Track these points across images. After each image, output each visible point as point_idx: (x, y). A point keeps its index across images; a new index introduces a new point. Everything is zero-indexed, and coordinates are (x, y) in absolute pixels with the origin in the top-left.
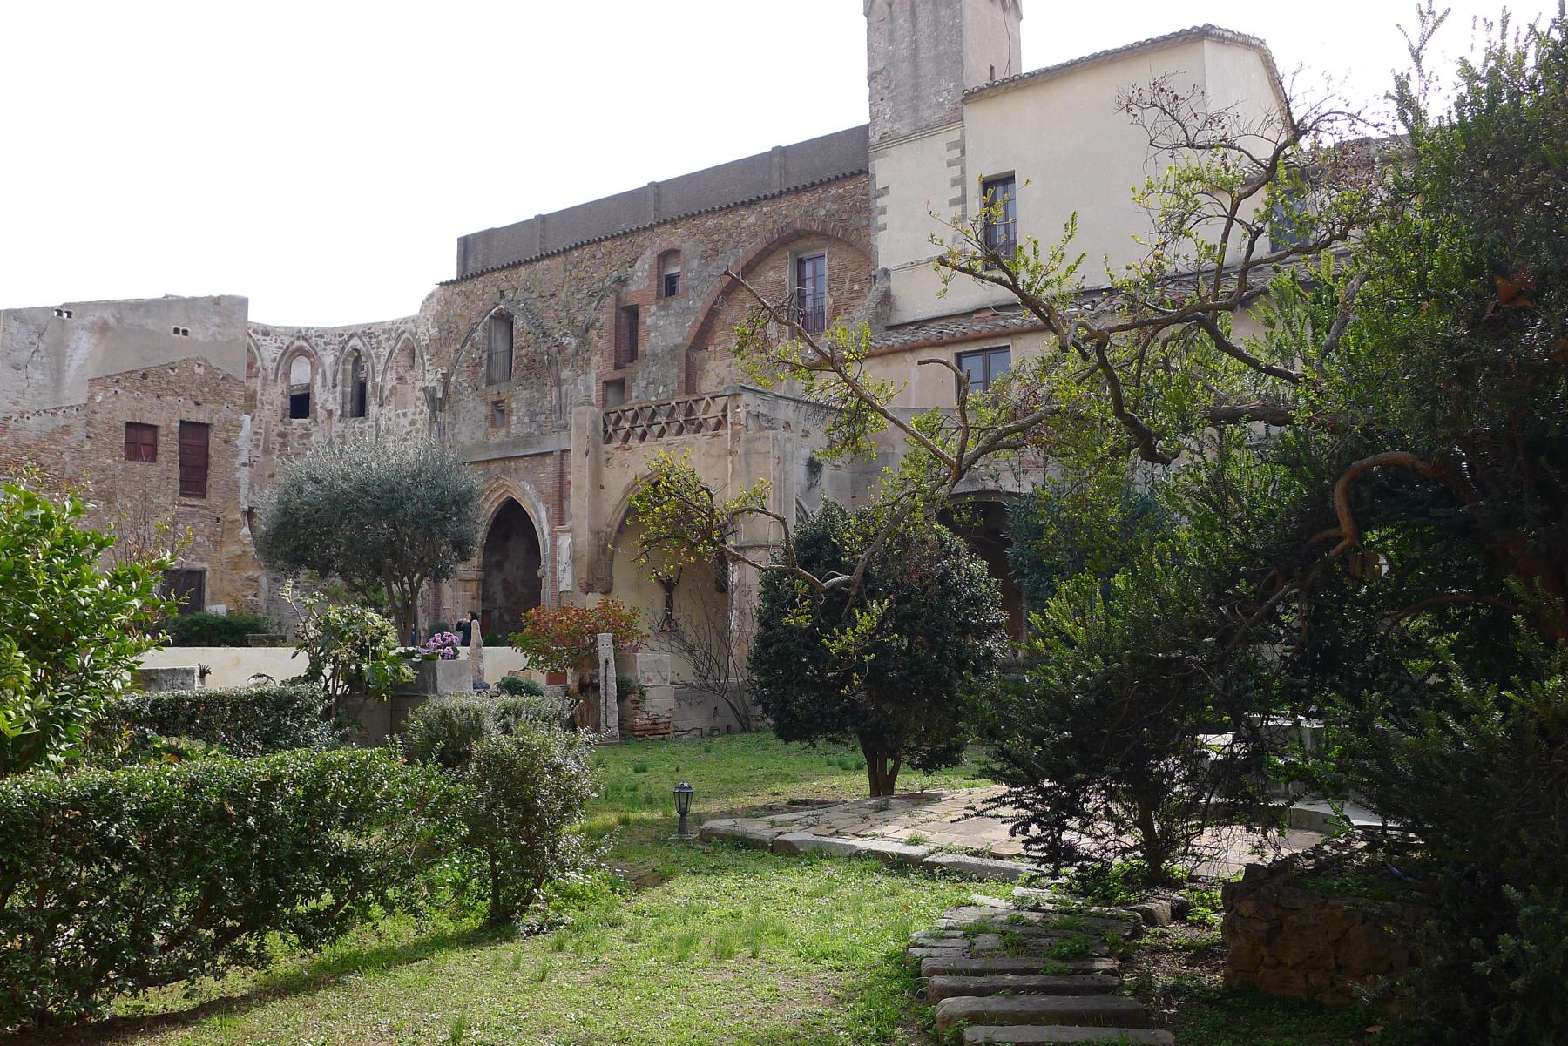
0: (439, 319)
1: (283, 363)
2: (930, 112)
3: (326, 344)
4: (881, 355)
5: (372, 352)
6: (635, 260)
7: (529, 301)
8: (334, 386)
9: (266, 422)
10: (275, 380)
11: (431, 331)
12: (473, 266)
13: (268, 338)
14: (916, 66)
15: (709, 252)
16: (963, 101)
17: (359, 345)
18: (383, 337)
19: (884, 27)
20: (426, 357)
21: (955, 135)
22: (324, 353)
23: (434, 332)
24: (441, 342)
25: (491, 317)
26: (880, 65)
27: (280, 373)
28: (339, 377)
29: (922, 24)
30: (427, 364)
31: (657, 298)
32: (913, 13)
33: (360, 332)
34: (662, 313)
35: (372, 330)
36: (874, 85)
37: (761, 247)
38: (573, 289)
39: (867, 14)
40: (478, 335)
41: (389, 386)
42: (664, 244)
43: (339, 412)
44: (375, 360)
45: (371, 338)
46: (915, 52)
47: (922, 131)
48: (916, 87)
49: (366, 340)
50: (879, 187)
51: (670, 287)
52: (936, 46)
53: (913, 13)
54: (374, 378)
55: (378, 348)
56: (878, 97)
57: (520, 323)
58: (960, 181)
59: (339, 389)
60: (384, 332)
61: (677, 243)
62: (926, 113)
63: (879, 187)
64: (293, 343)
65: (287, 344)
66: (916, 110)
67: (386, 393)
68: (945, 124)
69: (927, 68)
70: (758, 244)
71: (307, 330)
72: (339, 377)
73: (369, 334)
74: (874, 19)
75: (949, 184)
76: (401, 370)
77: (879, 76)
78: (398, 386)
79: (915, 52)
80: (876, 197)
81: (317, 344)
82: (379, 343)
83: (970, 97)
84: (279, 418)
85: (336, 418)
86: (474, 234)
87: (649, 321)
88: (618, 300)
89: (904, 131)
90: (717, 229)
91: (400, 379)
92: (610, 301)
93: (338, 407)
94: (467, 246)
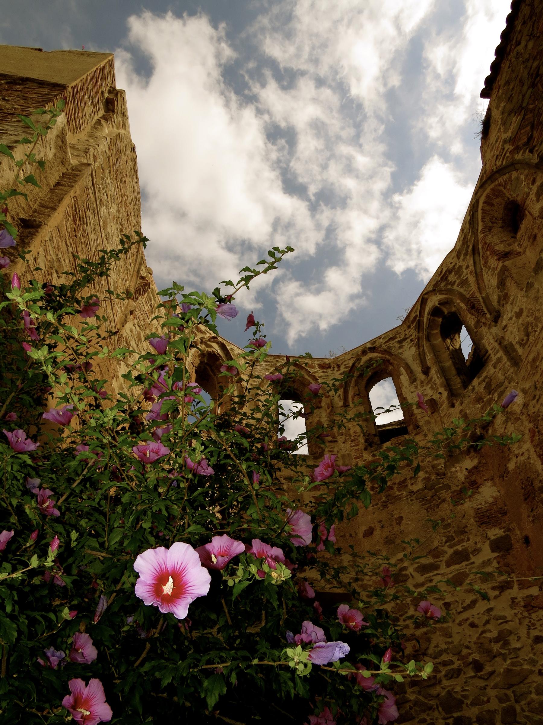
1: (353, 384)
3: (400, 342)
8: (426, 371)
9: (343, 456)
10: (346, 405)
13: (329, 370)
22: (401, 351)
27: (350, 395)
28: (429, 357)
43: (445, 394)
59: (433, 371)
64: (358, 359)
65: (351, 365)
71: (373, 342)
72: (429, 357)
81: (389, 348)
84: (361, 446)
85: (445, 406)
93: (441, 390)
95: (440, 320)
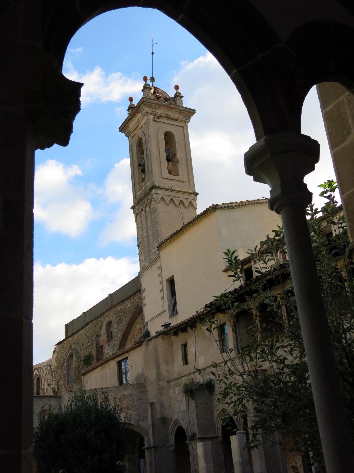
0: (58, 360)
2: (153, 256)
4: (101, 365)
5: (41, 375)
6: (101, 327)
7: (77, 348)
11: (54, 364)
12: (69, 334)
14: (148, 239)
15: (119, 320)
16: (158, 250)
17: (38, 373)
18: (44, 369)
19: (140, 225)
20: (54, 375)
21: (158, 264)
23: (55, 364)
24: (57, 368)
25: (68, 356)
26: (140, 241)
29: (149, 221)
30: (54, 378)
31: (107, 342)
32: (146, 219)
33: (37, 367)
34: (109, 348)
35: (41, 366)
36: (139, 248)
37: (131, 316)
38: (87, 342)
39: (136, 221)
40: (65, 364)
41: (46, 389)
42: (108, 319)
44: (42, 378)
45: (41, 369)
46: (148, 233)
47: (152, 263)
48: (149, 247)
49: (39, 370)
50: (143, 288)
51: (110, 336)
52: (152, 230)
53: (146, 219)
54: (42, 385)
55: (43, 373)
56: (140, 253)
57: (75, 357)
58: (161, 282)
60: (45, 366)
61: (111, 318)
62: (152, 257)
63: (143, 288)
66: (149, 256)
67: (45, 391)
68: (156, 259)
69: (151, 238)
70: (130, 315)
73: (40, 368)
74: (138, 223)
75: (159, 283)
76: (49, 381)
77: (140, 245)
78: (48, 388)
79: (148, 235)
80: (143, 293)
82: (43, 371)
83: (159, 247)
86: (69, 323)
87: (106, 352)
88: (97, 344)
89: (147, 265)
90: (121, 309)
91: (49, 385)
92: (94, 345)
94: (67, 326)
95: (37, 376)
